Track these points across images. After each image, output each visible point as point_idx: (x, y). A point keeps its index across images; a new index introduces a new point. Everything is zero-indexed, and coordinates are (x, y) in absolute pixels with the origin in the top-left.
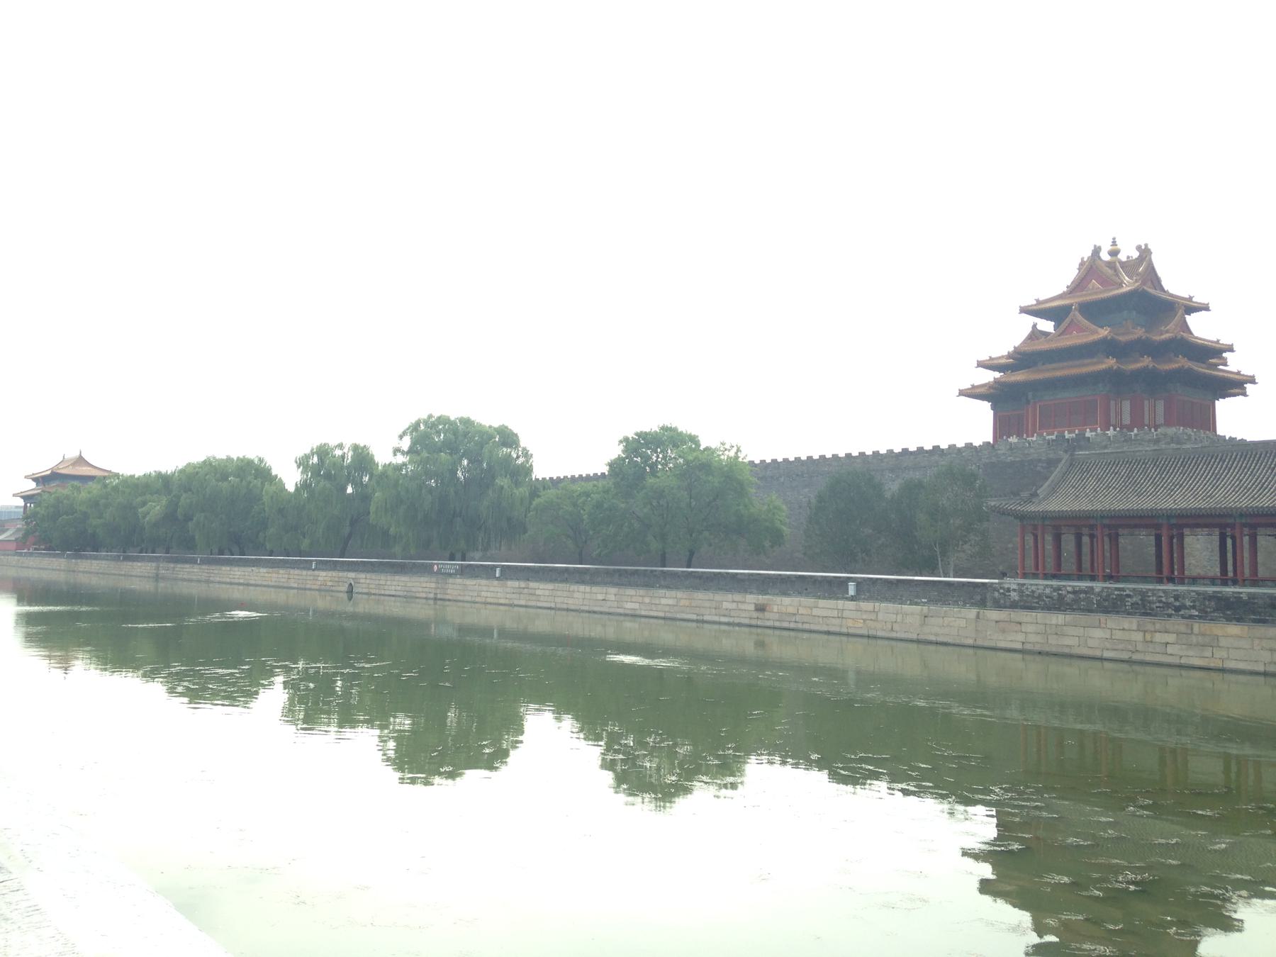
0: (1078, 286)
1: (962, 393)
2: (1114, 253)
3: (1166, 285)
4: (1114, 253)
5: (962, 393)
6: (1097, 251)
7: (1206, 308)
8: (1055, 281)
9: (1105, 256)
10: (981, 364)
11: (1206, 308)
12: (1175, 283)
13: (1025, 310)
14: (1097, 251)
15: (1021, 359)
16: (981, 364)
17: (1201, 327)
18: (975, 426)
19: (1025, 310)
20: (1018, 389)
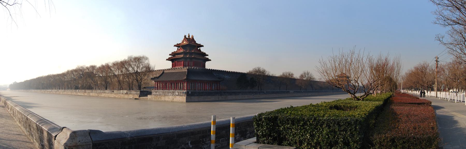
0: (183, 42)
1: (167, 60)
2: (189, 36)
3: (197, 42)
4: (189, 36)
5: (167, 60)
6: (185, 36)
7: (203, 46)
8: (180, 40)
9: (187, 37)
10: (170, 55)
11: (203, 46)
12: (198, 42)
13: (175, 46)
14: (185, 36)
15: (174, 54)
16: (170, 55)
17: (202, 49)
18: (169, 65)
19: (175, 46)
20: (173, 58)
